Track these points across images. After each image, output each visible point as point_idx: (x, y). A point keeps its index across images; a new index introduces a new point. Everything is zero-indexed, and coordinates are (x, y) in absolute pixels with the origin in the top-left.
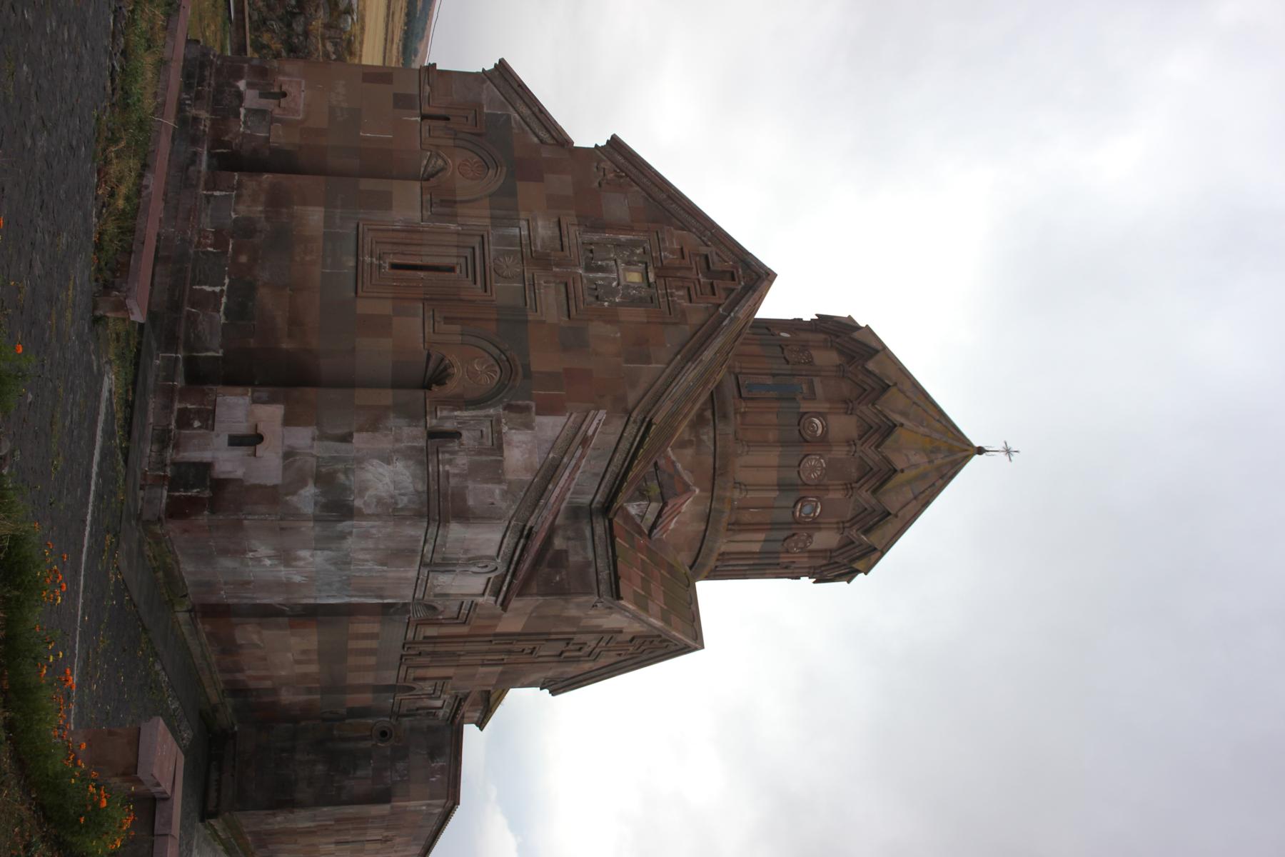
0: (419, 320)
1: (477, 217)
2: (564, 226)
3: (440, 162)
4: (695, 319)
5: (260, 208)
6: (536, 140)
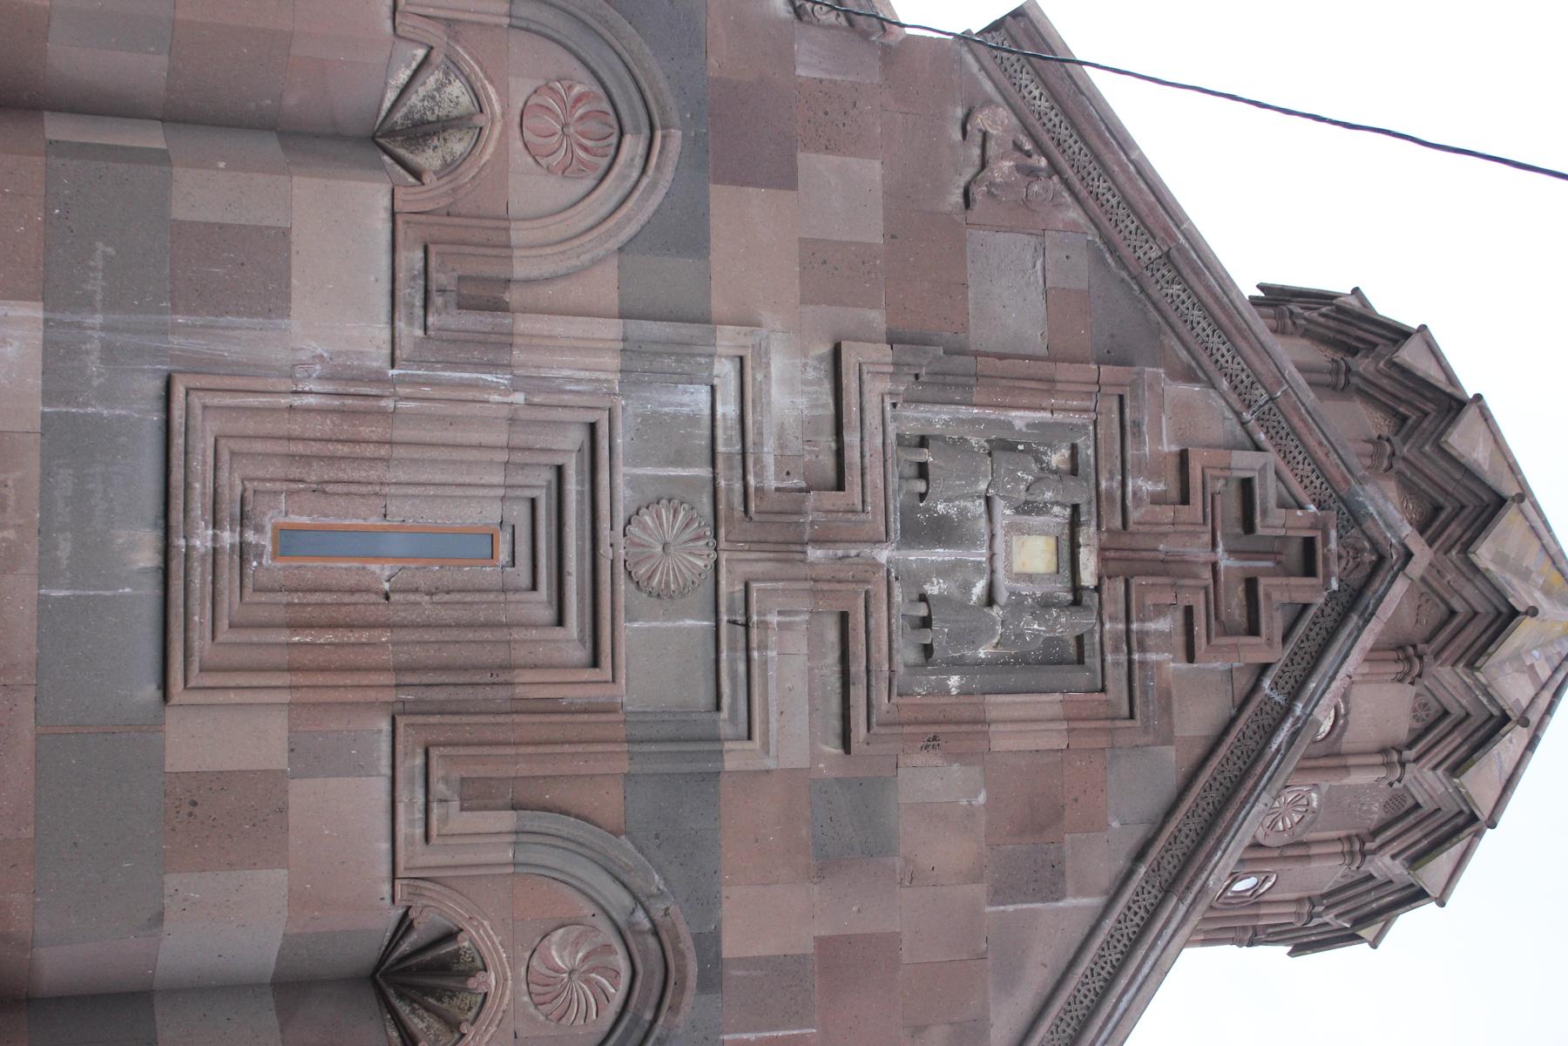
1: (574, 355)
3: (456, 89)
4: (1197, 717)
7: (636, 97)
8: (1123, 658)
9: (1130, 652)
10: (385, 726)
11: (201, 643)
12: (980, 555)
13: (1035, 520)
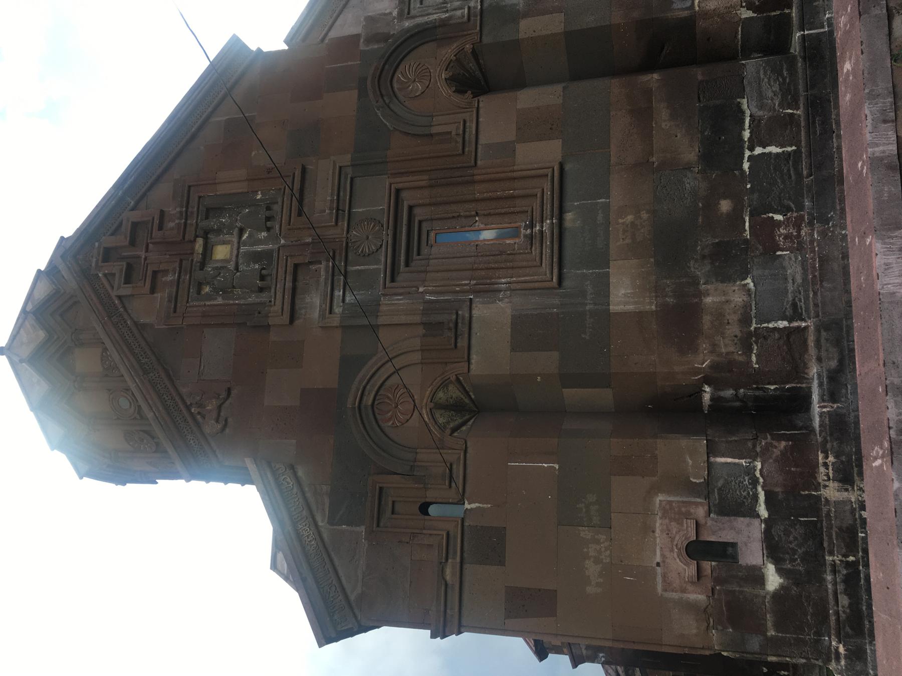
0: (483, 140)
2: (287, 307)
3: (441, 420)
5: (708, 300)
6: (300, 473)
7: (366, 422)
8: (190, 209)
9: (186, 211)
10: (479, 162)
11: (547, 186)
12: (243, 249)
13: (219, 265)
